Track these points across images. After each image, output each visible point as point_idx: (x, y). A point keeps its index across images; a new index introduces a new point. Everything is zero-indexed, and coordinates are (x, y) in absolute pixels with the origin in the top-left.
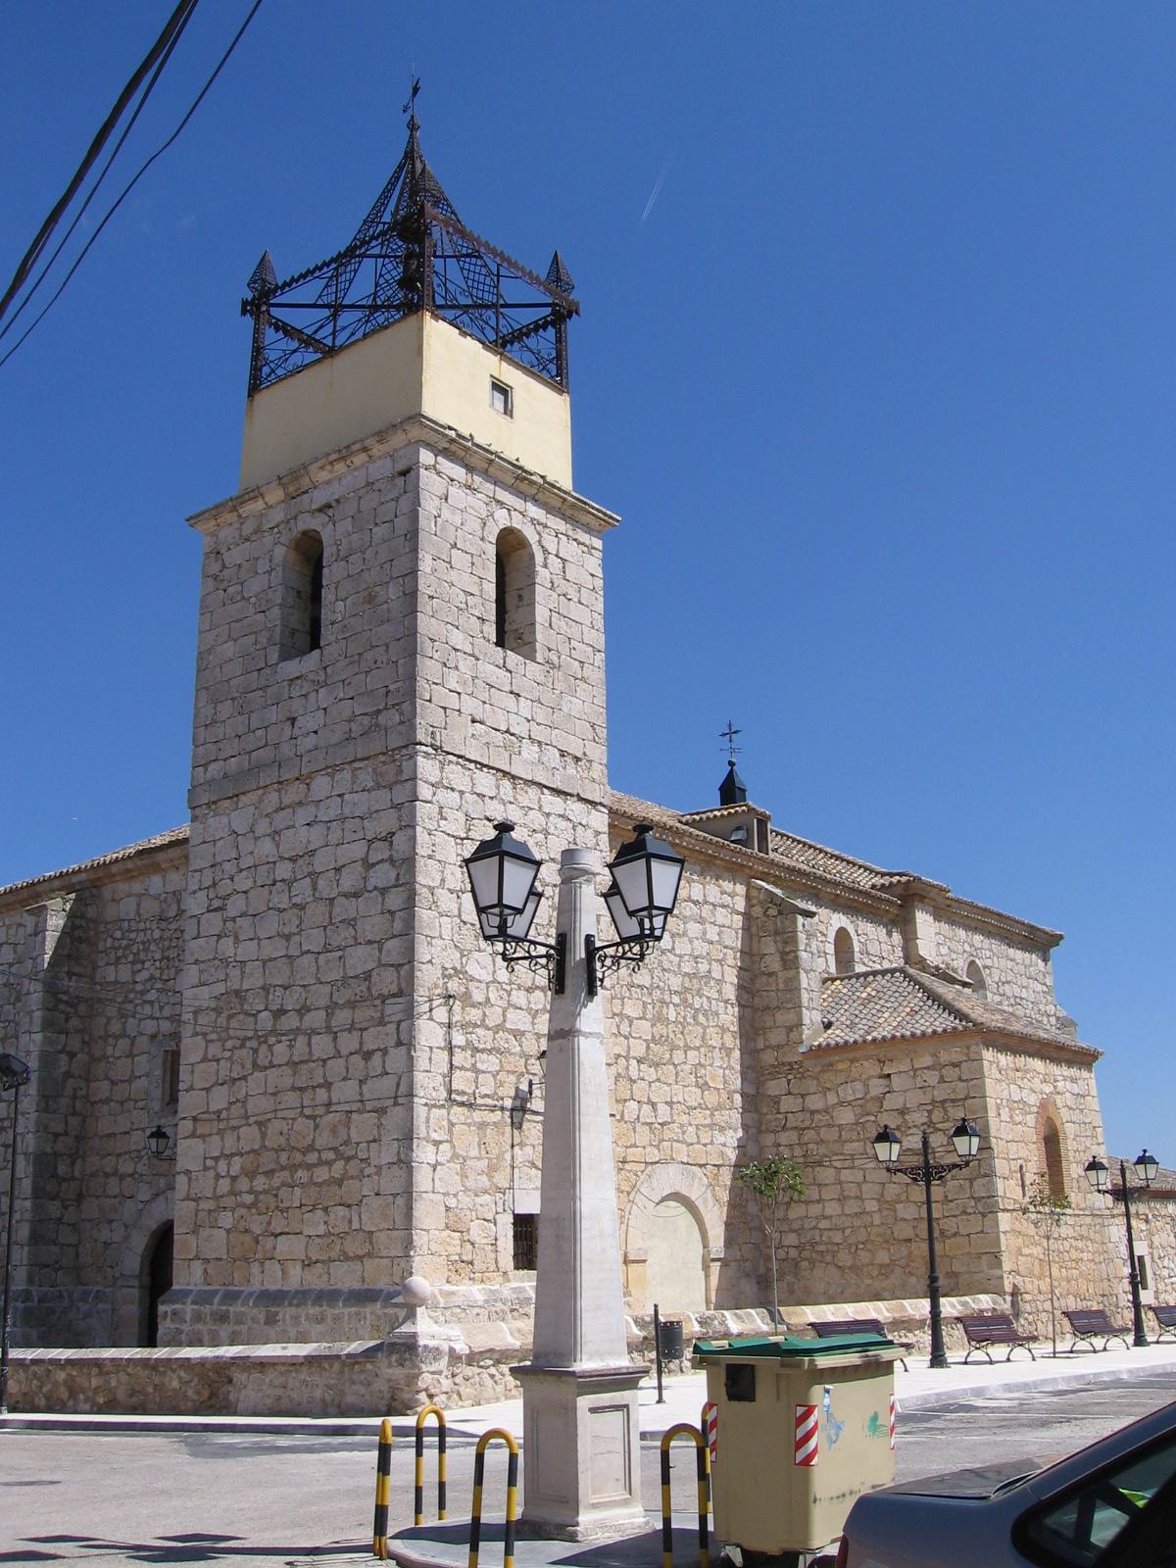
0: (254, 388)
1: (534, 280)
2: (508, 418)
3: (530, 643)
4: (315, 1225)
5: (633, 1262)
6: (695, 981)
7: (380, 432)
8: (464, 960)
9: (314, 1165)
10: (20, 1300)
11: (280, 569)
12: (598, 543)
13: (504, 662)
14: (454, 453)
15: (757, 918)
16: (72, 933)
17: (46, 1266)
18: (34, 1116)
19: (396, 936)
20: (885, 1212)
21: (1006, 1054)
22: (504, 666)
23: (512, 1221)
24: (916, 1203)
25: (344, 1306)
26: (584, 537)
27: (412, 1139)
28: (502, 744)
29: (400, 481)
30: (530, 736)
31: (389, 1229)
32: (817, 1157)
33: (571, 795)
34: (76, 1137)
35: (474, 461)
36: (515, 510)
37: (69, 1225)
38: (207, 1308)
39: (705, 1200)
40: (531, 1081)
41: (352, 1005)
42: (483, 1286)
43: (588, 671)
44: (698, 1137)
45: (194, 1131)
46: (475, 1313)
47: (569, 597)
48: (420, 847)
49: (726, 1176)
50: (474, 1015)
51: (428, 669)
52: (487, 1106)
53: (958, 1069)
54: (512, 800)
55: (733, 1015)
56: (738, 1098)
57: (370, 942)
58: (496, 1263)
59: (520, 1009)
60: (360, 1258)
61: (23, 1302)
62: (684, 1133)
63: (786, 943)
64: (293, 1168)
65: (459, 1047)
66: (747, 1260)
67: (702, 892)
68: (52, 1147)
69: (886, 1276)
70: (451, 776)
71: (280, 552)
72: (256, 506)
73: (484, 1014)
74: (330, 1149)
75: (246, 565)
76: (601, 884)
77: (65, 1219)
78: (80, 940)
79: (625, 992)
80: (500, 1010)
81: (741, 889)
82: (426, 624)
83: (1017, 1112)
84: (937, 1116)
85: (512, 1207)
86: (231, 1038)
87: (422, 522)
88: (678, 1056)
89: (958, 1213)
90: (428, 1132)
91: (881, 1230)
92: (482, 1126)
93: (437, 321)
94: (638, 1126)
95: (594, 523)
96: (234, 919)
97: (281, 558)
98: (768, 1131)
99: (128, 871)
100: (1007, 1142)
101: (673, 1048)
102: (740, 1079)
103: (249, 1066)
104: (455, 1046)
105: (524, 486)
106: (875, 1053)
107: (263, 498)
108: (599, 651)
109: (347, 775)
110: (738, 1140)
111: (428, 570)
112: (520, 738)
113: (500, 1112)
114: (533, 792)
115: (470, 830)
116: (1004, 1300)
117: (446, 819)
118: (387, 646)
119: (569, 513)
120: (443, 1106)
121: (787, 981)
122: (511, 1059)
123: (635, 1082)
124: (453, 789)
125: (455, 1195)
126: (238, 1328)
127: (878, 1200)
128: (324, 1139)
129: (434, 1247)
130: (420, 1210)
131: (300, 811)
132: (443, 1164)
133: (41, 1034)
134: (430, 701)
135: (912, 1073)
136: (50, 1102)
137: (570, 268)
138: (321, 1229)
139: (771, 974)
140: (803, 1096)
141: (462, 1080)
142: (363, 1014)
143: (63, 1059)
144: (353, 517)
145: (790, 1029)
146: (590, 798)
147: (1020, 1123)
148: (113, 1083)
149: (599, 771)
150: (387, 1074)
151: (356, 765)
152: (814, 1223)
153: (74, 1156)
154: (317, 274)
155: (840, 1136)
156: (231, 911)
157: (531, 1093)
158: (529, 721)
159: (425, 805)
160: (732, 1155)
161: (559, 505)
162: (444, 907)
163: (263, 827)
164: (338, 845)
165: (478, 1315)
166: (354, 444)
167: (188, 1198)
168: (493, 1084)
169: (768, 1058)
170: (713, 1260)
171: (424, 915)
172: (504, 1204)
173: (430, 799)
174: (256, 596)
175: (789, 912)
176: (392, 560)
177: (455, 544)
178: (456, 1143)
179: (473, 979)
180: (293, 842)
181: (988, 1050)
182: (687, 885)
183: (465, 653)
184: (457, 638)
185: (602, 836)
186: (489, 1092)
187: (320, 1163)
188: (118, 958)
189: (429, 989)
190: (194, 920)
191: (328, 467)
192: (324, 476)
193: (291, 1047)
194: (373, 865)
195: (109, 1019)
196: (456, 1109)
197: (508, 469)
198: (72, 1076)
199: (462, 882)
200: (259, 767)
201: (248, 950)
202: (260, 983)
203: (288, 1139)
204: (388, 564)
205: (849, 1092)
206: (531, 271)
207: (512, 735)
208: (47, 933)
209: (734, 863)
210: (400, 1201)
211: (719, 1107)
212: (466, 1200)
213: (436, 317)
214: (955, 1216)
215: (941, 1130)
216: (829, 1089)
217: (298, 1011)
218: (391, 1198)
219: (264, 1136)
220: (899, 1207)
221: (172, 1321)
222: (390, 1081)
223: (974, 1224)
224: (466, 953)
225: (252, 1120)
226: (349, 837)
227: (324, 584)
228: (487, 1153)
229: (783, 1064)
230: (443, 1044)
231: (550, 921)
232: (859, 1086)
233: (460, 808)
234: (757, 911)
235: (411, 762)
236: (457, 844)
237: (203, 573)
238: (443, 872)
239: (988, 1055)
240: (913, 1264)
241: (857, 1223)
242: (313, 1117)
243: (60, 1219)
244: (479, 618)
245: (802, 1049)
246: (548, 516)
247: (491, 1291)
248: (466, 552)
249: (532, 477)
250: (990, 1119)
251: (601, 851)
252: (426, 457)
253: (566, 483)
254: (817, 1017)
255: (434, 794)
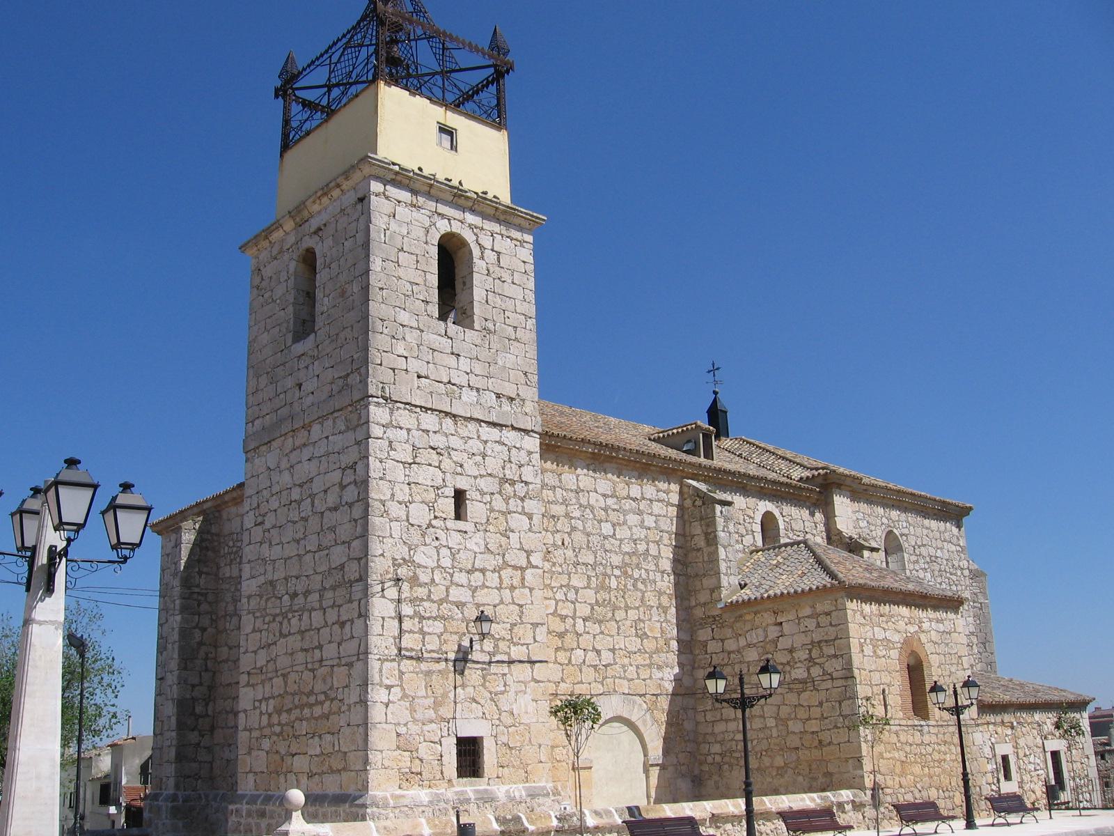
0: (286, 146)
1: (474, 49)
2: (453, 152)
3: (470, 316)
4: (314, 747)
5: (582, 768)
6: (634, 558)
7: (346, 172)
8: (412, 554)
9: (313, 705)
10: (170, 800)
11: (293, 278)
12: (529, 238)
13: (446, 332)
14: (400, 182)
15: (688, 508)
16: (198, 545)
17: (189, 777)
18: (176, 673)
19: (357, 538)
20: (780, 727)
21: (871, 604)
22: (446, 335)
23: (456, 742)
24: (801, 720)
25: (328, 806)
26: (516, 234)
27: (368, 685)
28: (444, 392)
29: (359, 207)
30: (469, 384)
31: (355, 750)
32: (733, 687)
33: (506, 426)
34: (209, 687)
35: (417, 186)
36: (455, 219)
37: (205, 748)
38: (254, 807)
39: (645, 722)
40: (471, 639)
41: (334, 588)
42: (431, 790)
43: (520, 333)
44: (638, 674)
45: (248, 682)
46: (420, 810)
47: (503, 279)
48: (372, 472)
49: (664, 703)
50: (421, 592)
51: (378, 341)
52: (432, 658)
53: (829, 617)
54: (453, 432)
55: (669, 582)
56: (674, 645)
57: (344, 543)
58: (442, 773)
59: (462, 586)
60: (339, 771)
61: (172, 802)
62: (625, 671)
63: (708, 526)
64: (302, 707)
65: (408, 616)
66: (684, 764)
67: (640, 491)
68: (190, 694)
69: (782, 776)
70: (399, 419)
71: (293, 265)
72: (277, 235)
73: (430, 591)
74: (322, 693)
75: (274, 277)
76: (533, 490)
77: (202, 744)
78: (207, 549)
79: (572, 569)
80: (444, 588)
81: (675, 487)
82: (375, 308)
83: (881, 648)
84: (815, 653)
85: (455, 732)
86: (267, 615)
87: (373, 234)
88: (620, 615)
89: (831, 727)
90: (381, 680)
91: (777, 741)
92: (428, 673)
93: (390, 87)
94: (584, 668)
95: (525, 224)
96: (269, 531)
97: (294, 270)
98: (699, 667)
99: (234, 499)
100: (870, 671)
101: (615, 609)
102: (676, 630)
103: (277, 634)
104: (404, 616)
105: (462, 201)
106: (771, 606)
107: (282, 228)
108: (530, 318)
109: (330, 422)
110: (674, 676)
111: (379, 269)
112: (461, 387)
113: (444, 663)
114: (472, 426)
115: (416, 457)
116: (865, 794)
117: (396, 450)
118: (352, 327)
119: (502, 218)
120: (394, 660)
121: (710, 554)
122: (454, 623)
123: (581, 635)
124: (401, 428)
125: (405, 725)
126: (270, 821)
127: (776, 718)
128: (319, 687)
129: (386, 763)
130: (375, 737)
131: (305, 450)
132: (394, 703)
133: (180, 616)
134: (381, 365)
135: (797, 621)
136: (188, 663)
137: (506, 37)
138: (318, 751)
139: (698, 550)
140: (722, 641)
141: (407, 641)
142: (341, 592)
143: (197, 634)
144: (333, 236)
145: (712, 591)
146: (522, 427)
147: (884, 657)
148: (230, 648)
149: (529, 407)
150: (353, 638)
151: (336, 415)
152: (732, 735)
153: (207, 700)
154: (317, 63)
155: (749, 670)
156: (268, 525)
157: (471, 647)
158: (468, 374)
159: (376, 440)
160: (670, 687)
161: (492, 212)
162: (393, 514)
163: (284, 464)
164: (325, 473)
165: (424, 812)
166: (330, 182)
167: (245, 729)
168: (438, 643)
169: (699, 613)
170: (652, 765)
171: (376, 521)
172: (448, 730)
173: (381, 436)
174: (280, 298)
175: (708, 501)
176: (355, 265)
177: (402, 249)
178: (405, 687)
179: (420, 566)
180: (301, 475)
181: (852, 601)
182: (626, 487)
183: (411, 327)
184: (404, 317)
185: (534, 455)
186: (434, 648)
187: (318, 703)
188: (231, 561)
189: (381, 575)
190: (248, 532)
191: (318, 201)
192: (316, 208)
193: (300, 620)
194: (345, 486)
195: (227, 603)
196: (405, 662)
197: (447, 190)
198: (205, 644)
199: (410, 495)
200: (281, 421)
201: (277, 552)
202: (283, 575)
203: (299, 687)
204: (353, 268)
205: (754, 637)
206: (470, 43)
207: (453, 385)
208: (182, 545)
209: (666, 468)
210: (361, 730)
211: (657, 651)
212: (414, 728)
213: (388, 84)
214: (828, 730)
215: (818, 664)
216: (740, 635)
217: (304, 594)
218: (356, 728)
219: (286, 683)
220: (790, 723)
221: (236, 816)
222: (355, 643)
223: (842, 736)
224: (413, 547)
225: (279, 673)
226: (332, 467)
227: (317, 286)
228: (433, 693)
229: (709, 617)
230: (393, 615)
231: (488, 520)
232: (760, 631)
233: (407, 441)
234: (688, 503)
235: (366, 411)
236: (404, 468)
237: (251, 284)
238: (392, 489)
239: (852, 606)
240: (800, 767)
241: (761, 735)
242: (313, 670)
243: (198, 744)
244: (423, 301)
245: (721, 605)
246: (484, 221)
247: (436, 794)
248: (412, 254)
249: (467, 194)
250: (852, 654)
251: (534, 466)
252: (376, 186)
253: (505, 198)
254: (735, 580)
255: (385, 432)
